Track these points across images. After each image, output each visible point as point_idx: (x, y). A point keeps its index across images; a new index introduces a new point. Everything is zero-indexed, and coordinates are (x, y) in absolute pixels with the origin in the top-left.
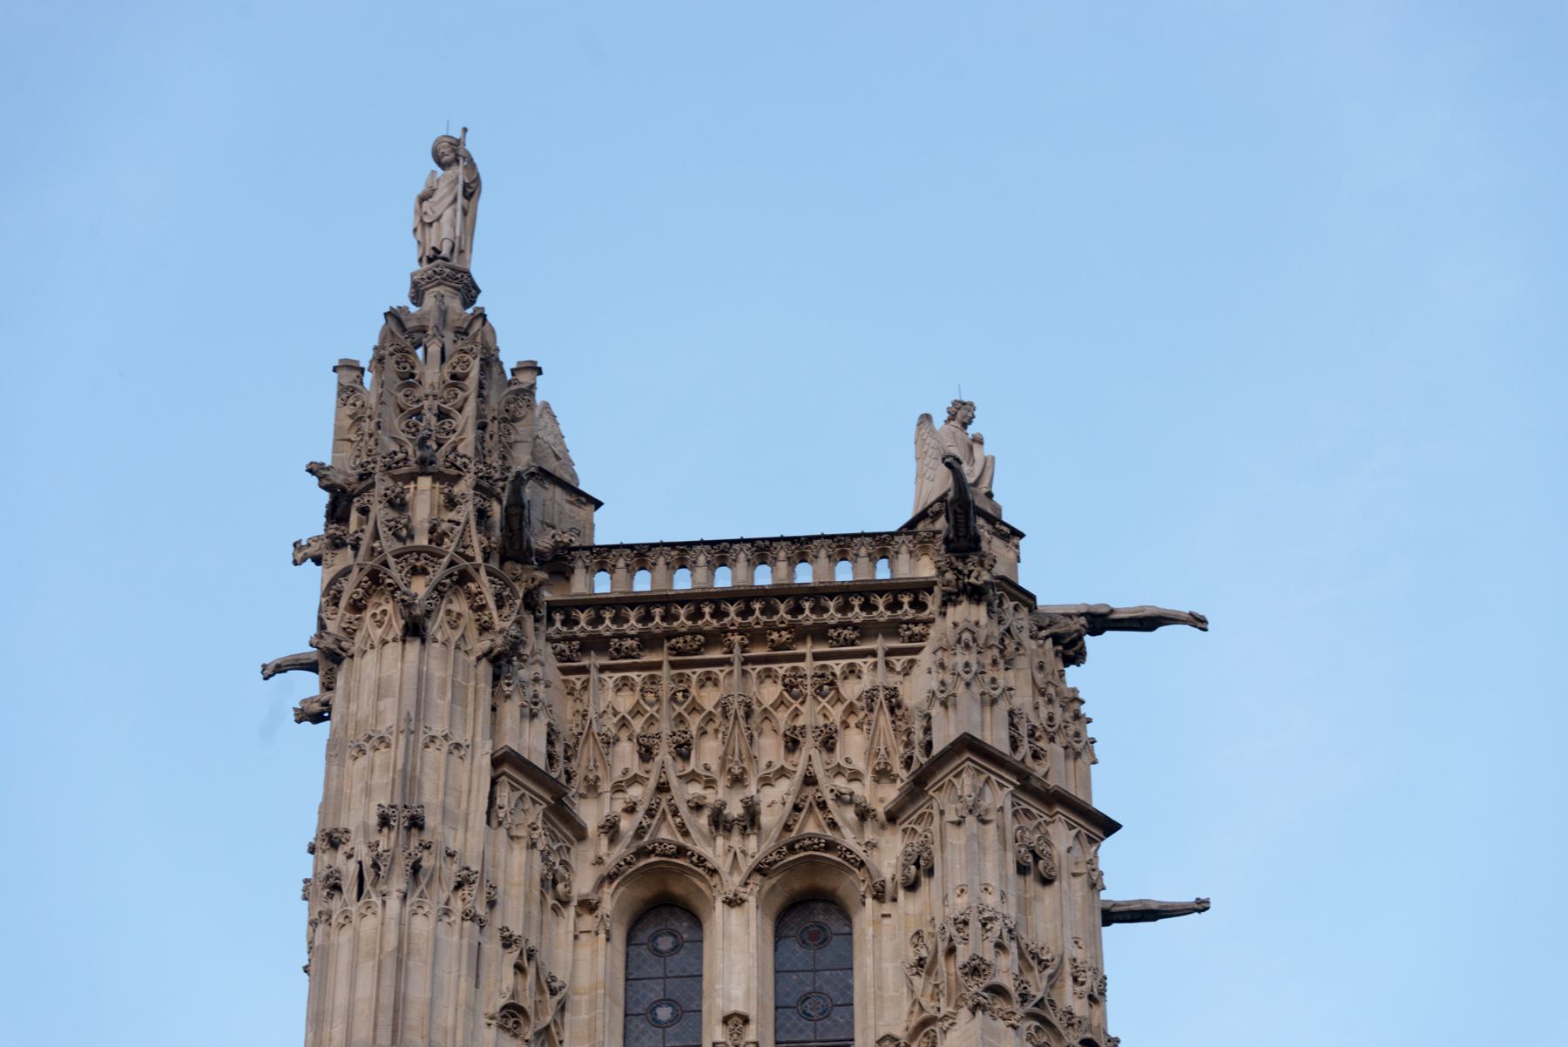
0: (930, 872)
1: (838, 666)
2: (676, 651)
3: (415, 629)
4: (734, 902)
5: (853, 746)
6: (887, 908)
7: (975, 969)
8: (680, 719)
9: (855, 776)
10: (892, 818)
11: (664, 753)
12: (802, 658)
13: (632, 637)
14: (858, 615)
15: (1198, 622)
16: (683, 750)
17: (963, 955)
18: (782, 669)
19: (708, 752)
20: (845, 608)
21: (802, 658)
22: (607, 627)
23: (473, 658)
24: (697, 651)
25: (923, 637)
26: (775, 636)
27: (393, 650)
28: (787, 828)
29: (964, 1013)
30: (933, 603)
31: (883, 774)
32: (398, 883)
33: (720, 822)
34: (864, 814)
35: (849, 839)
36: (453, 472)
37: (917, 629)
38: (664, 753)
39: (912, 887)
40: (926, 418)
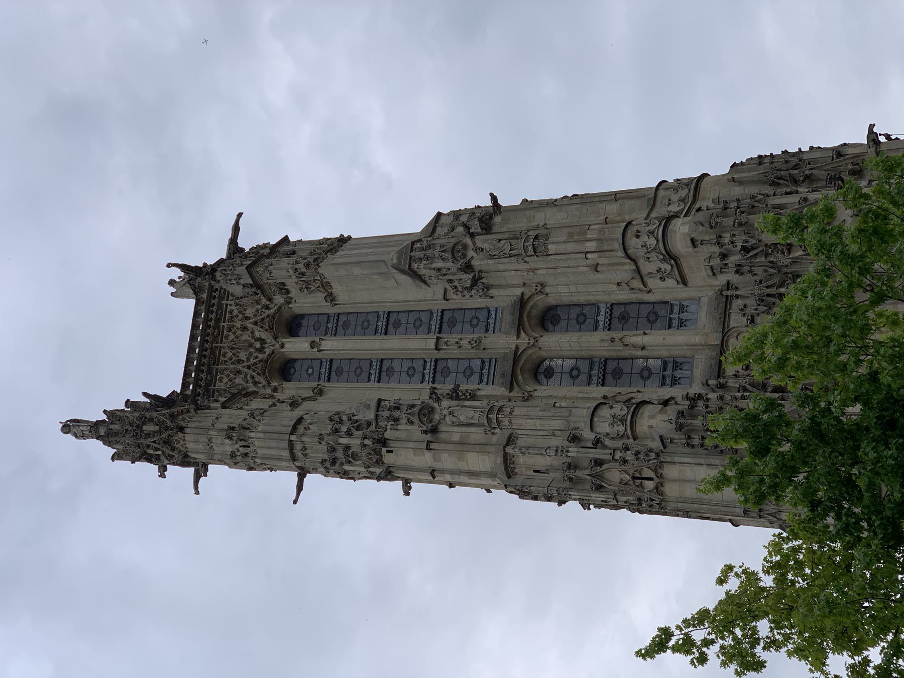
0: (283, 284)
3: (182, 429)
4: (283, 346)
5: (249, 312)
7: (307, 265)
8: (232, 363)
9: (257, 311)
10: (270, 299)
11: (240, 367)
14: (215, 309)
15: (240, 215)
16: (240, 361)
17: (304, 270)
19: (243, 356)
20: (212, 312)
22: (202, 384)
25: (225, 290)
27: (187, 437)
28: (266, 330)
30: (217, 286)
31: (258, 302)
32: (247, 433)
33: (261, 350)
34: (267, 308)
35: (272, 311)
38: (240, 367)
39: (288, 292)
40: (172, 294)
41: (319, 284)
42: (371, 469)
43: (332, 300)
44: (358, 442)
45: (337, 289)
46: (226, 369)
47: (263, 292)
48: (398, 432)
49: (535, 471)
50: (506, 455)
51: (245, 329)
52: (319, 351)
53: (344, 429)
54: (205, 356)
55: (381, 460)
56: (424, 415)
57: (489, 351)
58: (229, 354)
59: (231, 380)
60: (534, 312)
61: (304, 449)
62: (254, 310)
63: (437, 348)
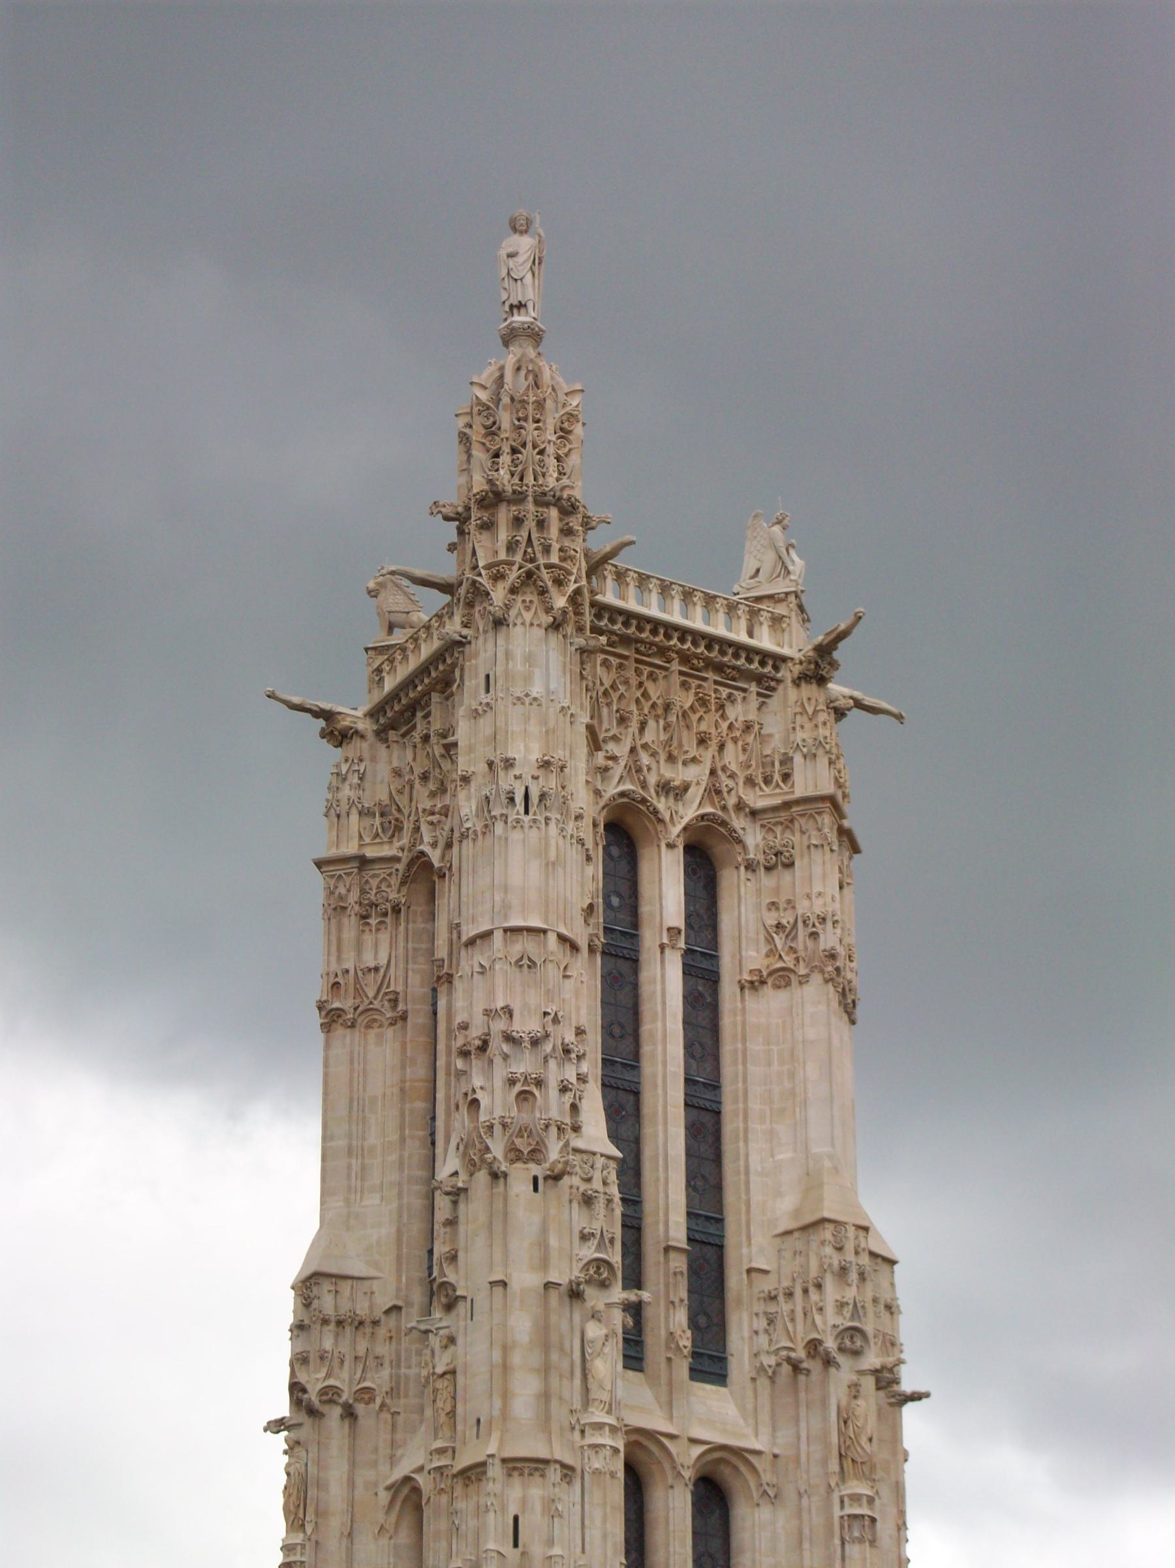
1: (725, 692)
2: (638, 651)
4: (671, 846)
6: (750, 875)
9: (732, 776)
11: (634, 726)
12: (705, 679)
13: (617, 635)
18: (695, 683)
21: (705, 679)
23: (573, 649)
24: (649, 656)
25: (773, 689)
26: (695, 662)
29: (817, 978)
30: (786, 673)
36: (570, 509)
37: (773, 684)
41: (789, 961)
42: (498, 1129)
43: (752, 982)
44: (554, 1114)
45: (772, 1001)
46: (626, 682)
47: (775, 809)
48: (567, 1204)
49: (516, 1519)
50: (546, 1462)
51: (702, 741)
52: (662, 947)
53: (571, 1074)
54: (654, 632)
55: (518, 1159)
56: (597, 1271)
57: (663, 1365)
58: (654, 691)
59: (606, 693)
60: (726, 1471)
61: (532, 964)
62: (733, 767)
63: (667, 1249)
